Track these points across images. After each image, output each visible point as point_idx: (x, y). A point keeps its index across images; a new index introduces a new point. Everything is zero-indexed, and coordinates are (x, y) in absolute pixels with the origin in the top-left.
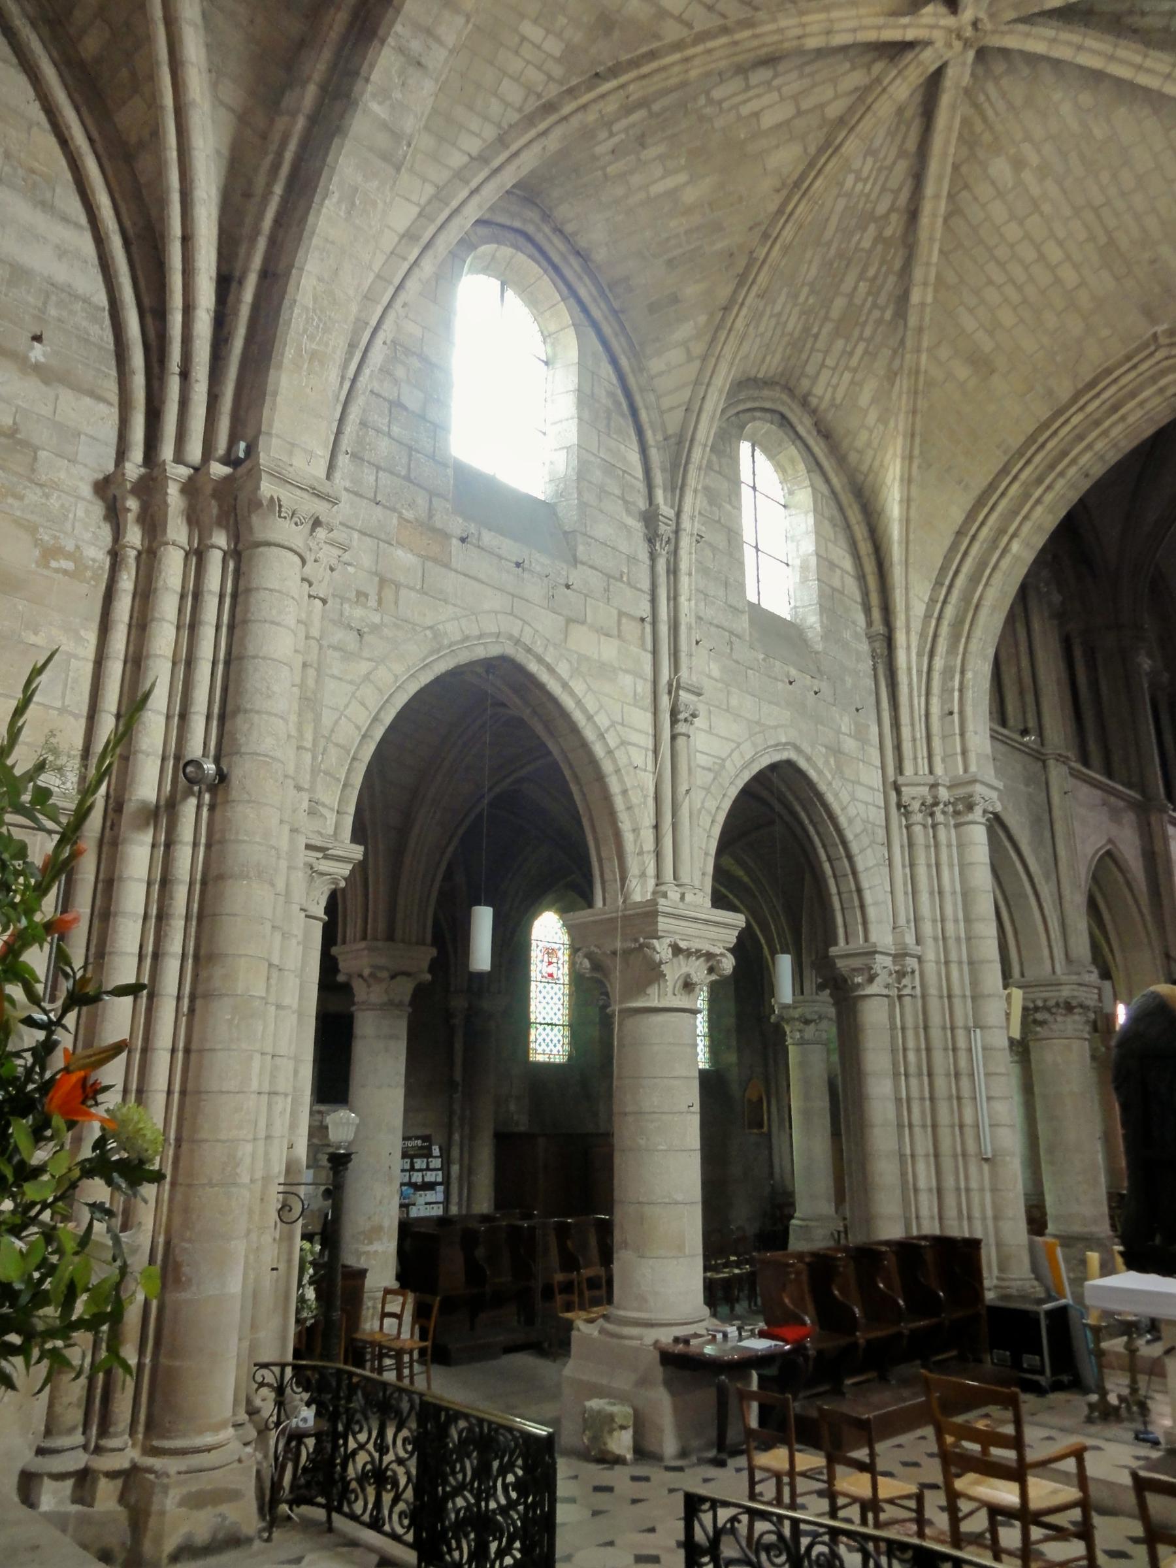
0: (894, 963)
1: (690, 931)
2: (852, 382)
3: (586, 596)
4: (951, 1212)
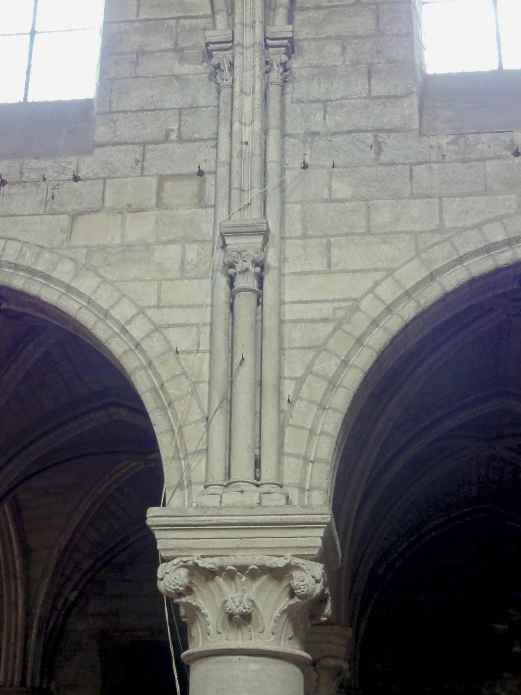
1: (219, 544)
3: (105, 179)
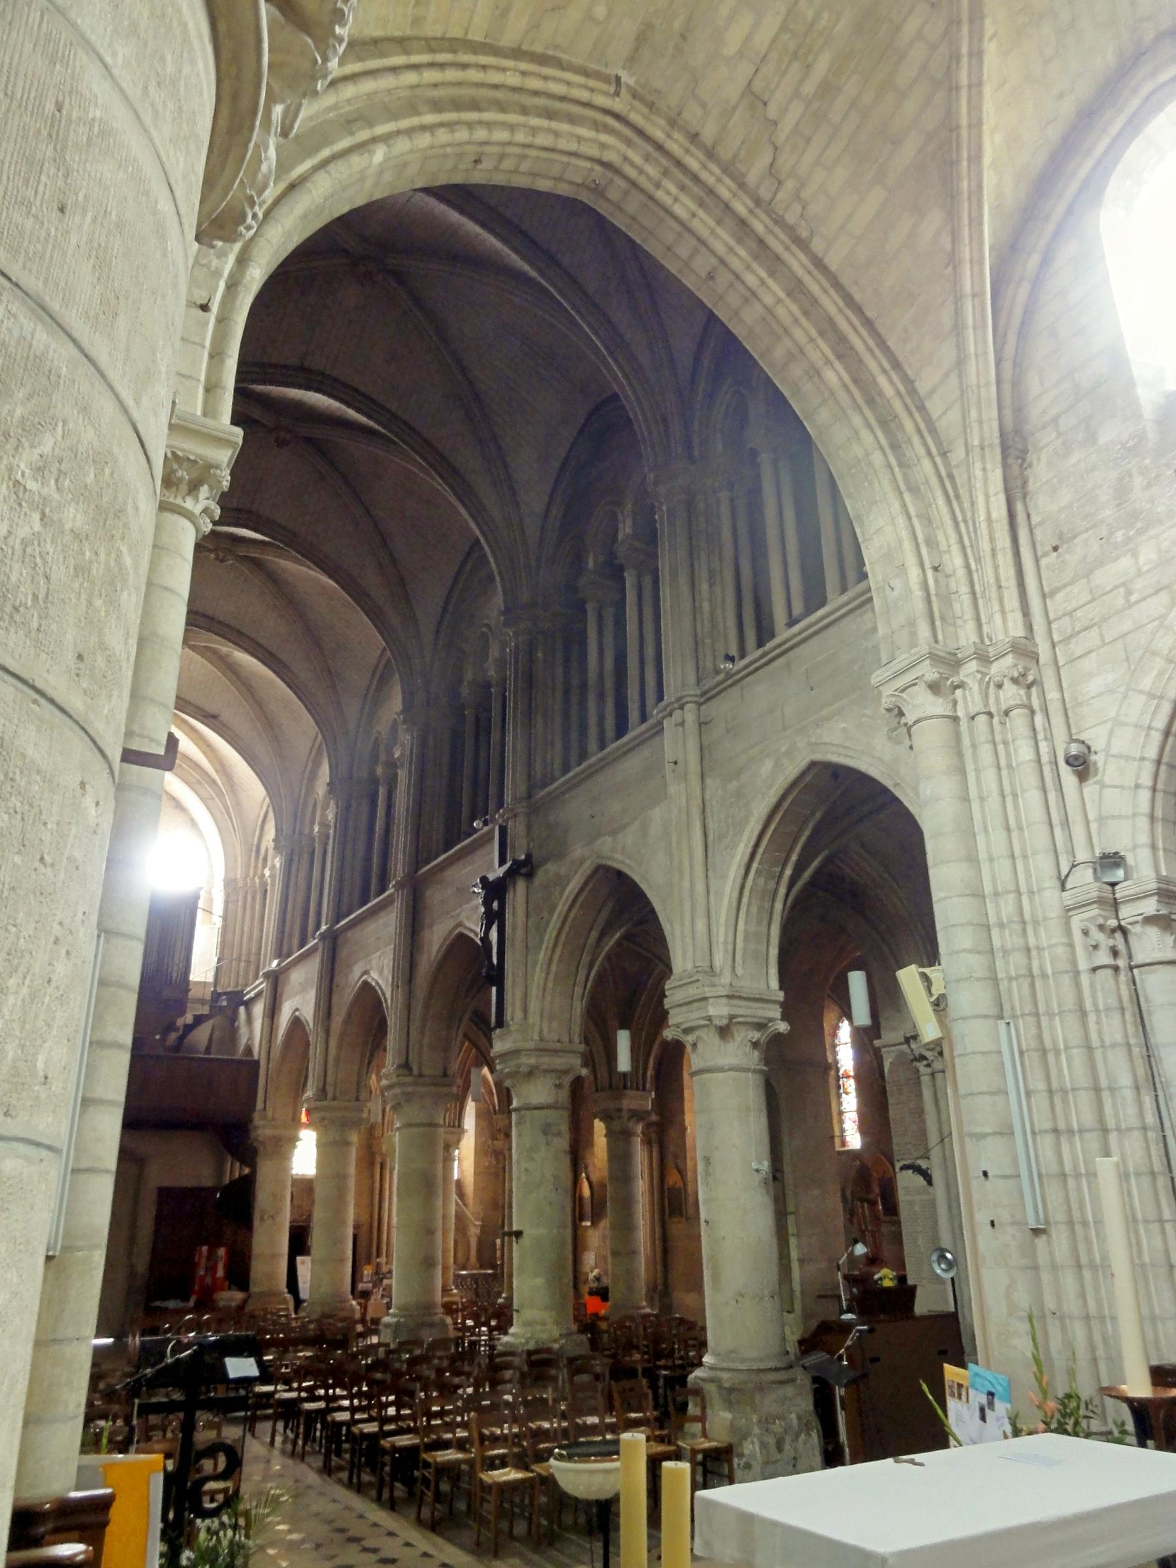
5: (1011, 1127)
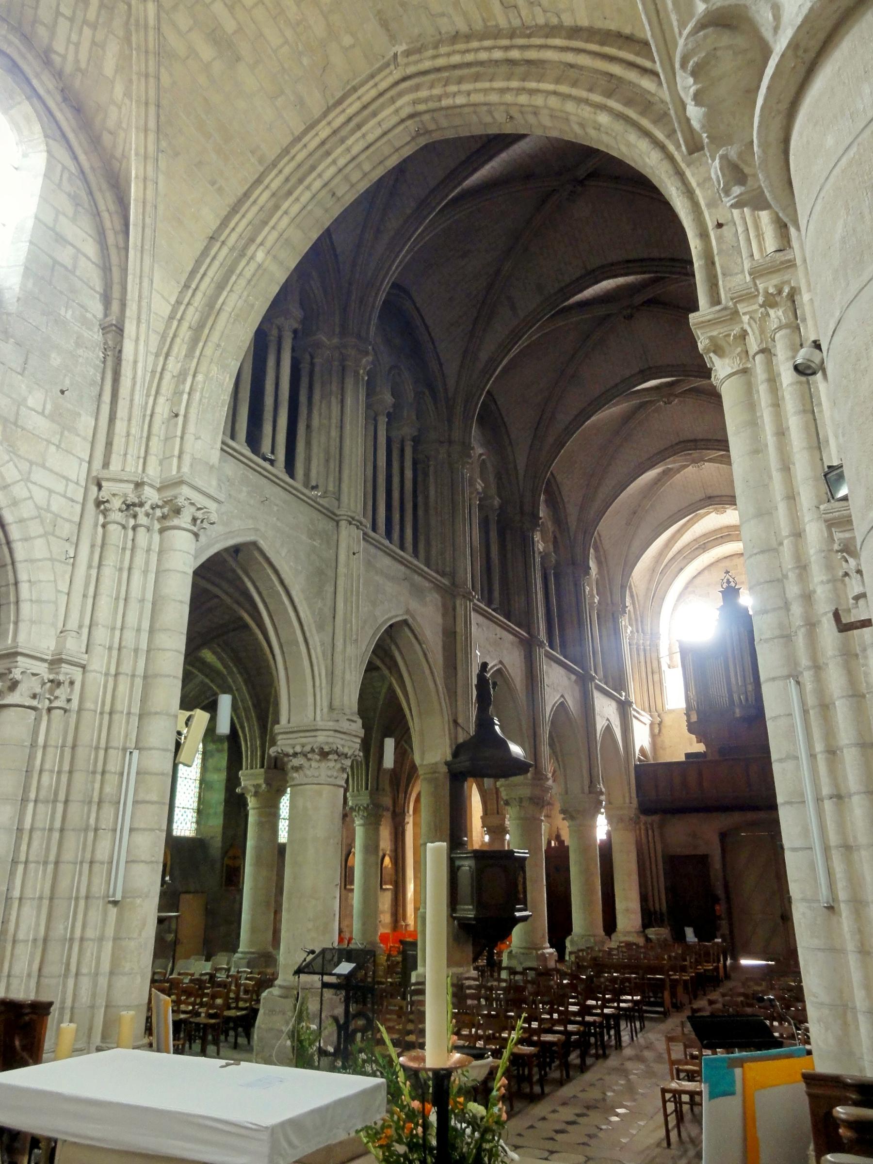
0: (51, 670)
2: (93, 43)
4: (54, 968)
5: (802, 795)
